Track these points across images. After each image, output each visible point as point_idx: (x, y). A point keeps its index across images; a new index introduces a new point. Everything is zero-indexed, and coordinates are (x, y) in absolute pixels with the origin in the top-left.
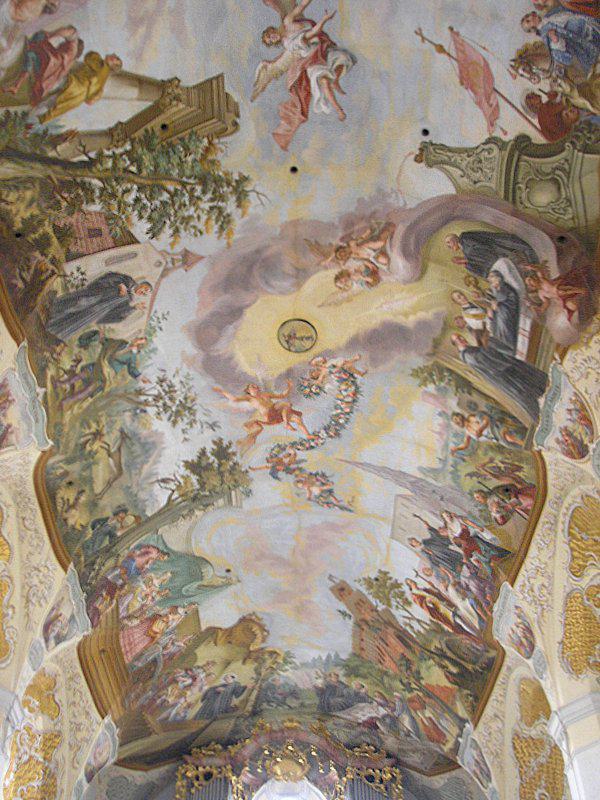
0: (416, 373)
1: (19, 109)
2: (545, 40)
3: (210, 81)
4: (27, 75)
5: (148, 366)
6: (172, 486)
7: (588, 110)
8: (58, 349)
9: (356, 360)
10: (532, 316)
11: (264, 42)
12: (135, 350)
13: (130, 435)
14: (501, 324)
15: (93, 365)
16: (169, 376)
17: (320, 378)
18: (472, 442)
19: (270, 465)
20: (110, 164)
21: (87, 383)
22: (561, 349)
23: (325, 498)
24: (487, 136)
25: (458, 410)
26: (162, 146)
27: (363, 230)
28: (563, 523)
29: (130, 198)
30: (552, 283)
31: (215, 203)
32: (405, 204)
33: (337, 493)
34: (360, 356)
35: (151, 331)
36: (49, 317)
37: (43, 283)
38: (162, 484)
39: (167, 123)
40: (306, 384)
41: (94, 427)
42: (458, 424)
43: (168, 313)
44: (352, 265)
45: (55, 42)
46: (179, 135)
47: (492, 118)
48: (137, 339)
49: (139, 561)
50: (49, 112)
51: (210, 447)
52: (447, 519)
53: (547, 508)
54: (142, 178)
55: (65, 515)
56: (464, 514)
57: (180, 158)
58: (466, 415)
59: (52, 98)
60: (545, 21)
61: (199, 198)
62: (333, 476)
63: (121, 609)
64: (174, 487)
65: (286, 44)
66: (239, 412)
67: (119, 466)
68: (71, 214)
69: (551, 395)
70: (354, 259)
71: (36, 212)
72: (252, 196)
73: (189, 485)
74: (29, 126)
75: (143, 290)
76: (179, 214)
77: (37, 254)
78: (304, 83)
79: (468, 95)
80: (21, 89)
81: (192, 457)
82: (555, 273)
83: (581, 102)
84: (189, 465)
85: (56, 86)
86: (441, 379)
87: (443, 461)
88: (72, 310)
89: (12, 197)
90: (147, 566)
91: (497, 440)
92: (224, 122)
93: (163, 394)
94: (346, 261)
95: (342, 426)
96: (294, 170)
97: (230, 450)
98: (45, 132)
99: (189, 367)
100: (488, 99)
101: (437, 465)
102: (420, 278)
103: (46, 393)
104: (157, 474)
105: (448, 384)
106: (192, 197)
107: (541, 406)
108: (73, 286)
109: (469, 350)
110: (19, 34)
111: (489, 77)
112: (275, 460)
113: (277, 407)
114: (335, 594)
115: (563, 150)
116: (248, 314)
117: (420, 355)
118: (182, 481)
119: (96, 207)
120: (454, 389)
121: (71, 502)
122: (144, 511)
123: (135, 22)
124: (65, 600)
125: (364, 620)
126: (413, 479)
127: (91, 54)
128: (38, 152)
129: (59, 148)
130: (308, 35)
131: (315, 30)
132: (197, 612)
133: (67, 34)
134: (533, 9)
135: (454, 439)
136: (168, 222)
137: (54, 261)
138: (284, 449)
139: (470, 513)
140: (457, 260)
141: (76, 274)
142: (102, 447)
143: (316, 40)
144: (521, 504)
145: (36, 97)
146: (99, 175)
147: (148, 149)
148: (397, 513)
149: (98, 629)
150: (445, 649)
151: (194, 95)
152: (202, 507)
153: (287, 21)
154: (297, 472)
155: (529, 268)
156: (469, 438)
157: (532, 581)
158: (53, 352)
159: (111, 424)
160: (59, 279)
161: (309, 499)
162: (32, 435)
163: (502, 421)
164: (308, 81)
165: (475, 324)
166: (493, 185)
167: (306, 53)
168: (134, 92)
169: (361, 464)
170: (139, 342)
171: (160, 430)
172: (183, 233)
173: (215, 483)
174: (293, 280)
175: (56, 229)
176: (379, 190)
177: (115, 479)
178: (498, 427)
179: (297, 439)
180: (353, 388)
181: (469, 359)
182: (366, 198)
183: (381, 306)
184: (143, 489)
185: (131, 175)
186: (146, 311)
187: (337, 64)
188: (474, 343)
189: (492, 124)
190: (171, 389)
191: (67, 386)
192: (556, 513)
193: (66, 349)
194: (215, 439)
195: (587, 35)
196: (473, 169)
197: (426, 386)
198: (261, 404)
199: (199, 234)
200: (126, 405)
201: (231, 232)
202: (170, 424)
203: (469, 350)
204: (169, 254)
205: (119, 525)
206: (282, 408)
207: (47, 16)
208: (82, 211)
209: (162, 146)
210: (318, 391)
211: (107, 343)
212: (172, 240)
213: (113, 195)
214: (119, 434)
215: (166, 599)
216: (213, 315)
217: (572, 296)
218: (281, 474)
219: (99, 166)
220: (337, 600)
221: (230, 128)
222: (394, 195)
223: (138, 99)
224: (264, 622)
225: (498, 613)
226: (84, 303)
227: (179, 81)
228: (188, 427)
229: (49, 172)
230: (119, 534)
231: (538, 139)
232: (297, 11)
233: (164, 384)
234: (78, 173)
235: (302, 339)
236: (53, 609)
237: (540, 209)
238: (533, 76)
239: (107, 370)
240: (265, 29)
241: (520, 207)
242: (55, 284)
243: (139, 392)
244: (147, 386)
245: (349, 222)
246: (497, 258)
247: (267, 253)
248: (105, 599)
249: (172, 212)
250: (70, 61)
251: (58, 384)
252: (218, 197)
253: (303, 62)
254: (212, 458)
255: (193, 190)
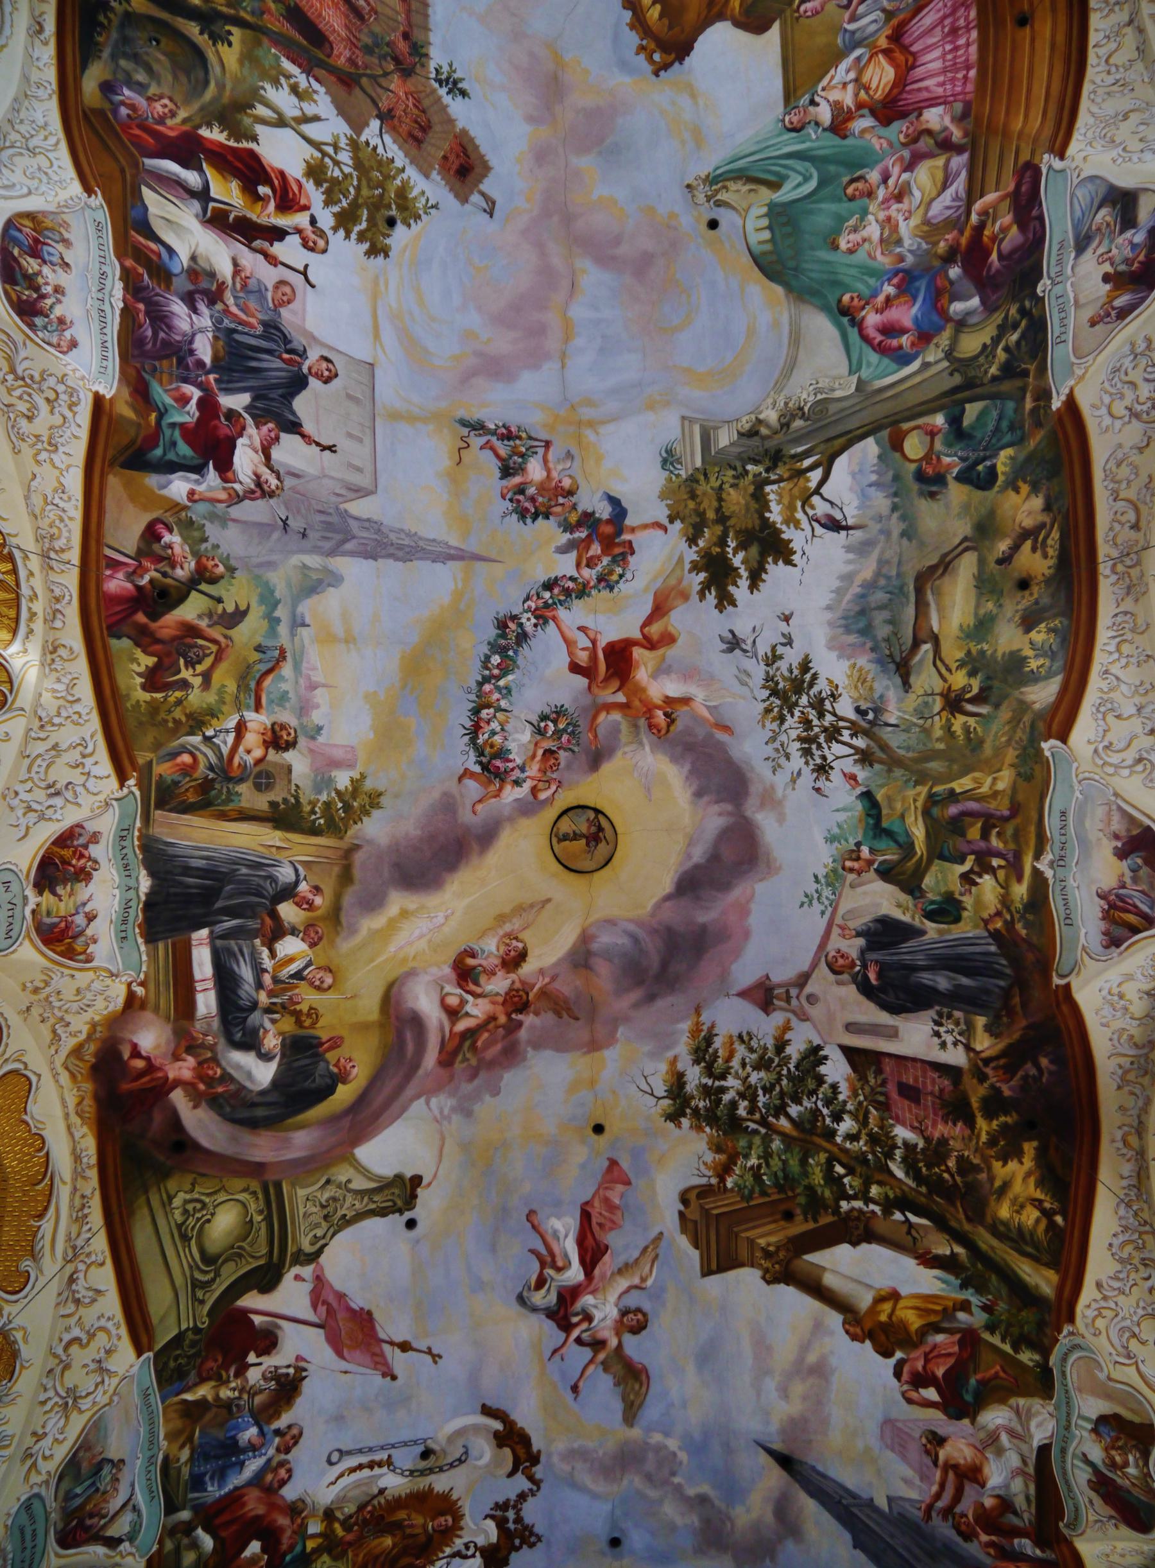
0: (374, 800)
1: (996, 1340)
2: (266, 1429)
3: (721, 1269)
4: (979, 1376)
5: (844, 809)
6: (820, 507)
7: (188, 1389)
8: (999, 924)
9: (480, 801)
10: (198, 1025)
11: (645, 1315)
12: (865, 851)
13: (892, 667)
14: (246, 973)
15: (942, 857)
16: (808, 777)
17: (540, 752)
18: (252, 702)
19: (626, 537)
20: (874, 1190)
21: (957, 825)
22: (137, 1004)
23: (515, 452)
24: (323, 1259)
25: (290, 756)
26: (793, 1190)
27: (488, 1045)
28: (31, 574)
29: (847, 1125)
30: (177, 1083)
31: (717, 1083)
32: (428, 1103)
33: (493, 466)
34: (474, 813)
35: (834, 879)
36: (1007, 994)
37: (1003, 1054)
38: (838, 516)
39: (782, 1223)
40: (565, 738)
41: (959, 722)
42: (283, 727)
43: (802, 905)
44: (499, 984)
45: (931, 1394)
46: (767, 1199)
47: (320, 1291)
48: (859, 873)
49: (907, 314)
50: (955, 1309)
51: (740, 591)
52: (266, 474)
53: (70, 580)
54: (826, 1151)
55: (1047, 519)
56: (236, 512)
57: (768, 1165)
58: (272, 755)
59: (946, 1325)
60: (271, 1451)
61: (742, 1095)
62: (504, 515)
63: (959, 185)
64: (816, 500)
65: (614, 1313)
66: (689, 674)
67: (921, 606)
68: (943, 1141)
69: (132, 911)
70: (497, 994)
71: (996, 1165)
72: (661, 1090)
73: (786, 501)
74: (985, 1308)
75: (841, 961)
76: (773, 1076)
77: (1007, 1092)
78: (588, 1260)
79: (358, 1301)
80: (991, 1368)
81: (776, 571)
82: (178, 1097)
83: (204, 1391)
84: (783, 552)
85: (940, 1338)
86: (328, 805)
87: (298, 623)
88: (965, 981)
89: (1031, 1216)
90: (889, 289)
91: (207, 740)
92: (702, 1207)
93: (822, 739)
94: (511, 990)
95: (495, 648)
96: (599, 1129)
97: (702, 576)
98: (964, 1286)
99: (772, 787)
100: (331, 1312)
101: (306, 608)
102: (390, 986)
103: (1037, 856)
104: (849, 549)
105: (313, 804)
106: (753, 1100)
107: (143, 872)
108: (957, 1024)
109: (288, 892)
110: (982, 1435)
111: (336, 1344)
112: (617, 551)
113: (616, 684)
114: (482, 157)
115: (209, 1314)
116: (667, 884)
117: (370, 842)
118: (799, 515)
119: (902, 1133)
120: (303, 800)
121: (1028, 544)
122: (880, 457)
123: (820, 1371)
124: (1088, 313)
125: (407, 72)
126: (348, 546)
127: (887, 1354)
128: (979, 1266)
129: (948, 1252)
130: (585, 1326)
131: (575, 1333)
132: (789, 95)
133: (913, 1395)
134: (289, 1457)
135: (284, 686)
136: (791, 1066)
137: (982, 1078)
138: (601, 579)
139: (223, 521)
140: (336, 1042)
141: (949, 1039)
142: (949, 670)
143: (575, 1320)
144: (130, 577)
145: (969, 1339)
146: (894, 1182)
147: (815, 1192)
148: (368, 440)
149: (1025, 156)
150: (202, 40)
151: (744, 1254)
152: (764, 431)
153: (613, 1342)
154: (573, 518)
155: (220, 1090)
156: (258, 707)
157: (57, 420)
158: (1009, 925)
159: (922, 712)
160: (978, 1048)
161: (548, 444)
162: (1077, 794)
163: (206, 786)
164: (582, 1261)
165: (290, 946)
166: (302, 1193)
167: (587, 1300)
168: (829, 1280)
169: (452, 558)
170: (856, 865)
171: (833, 655)
172: (770, 1043)
173: (731, 491)
174: (595, 946)
175: (970, 1123)
176: (468, 1114)
177: (933, 569)
178: (211, 768)
179: (578, 605)
180: (480, 741)
181: (285, 874)
182: (487, 1098)
183: (447, 917)
184: (879, 518)
185: (845, 1160)
186: (838, 920)
187: (543, 1291)
188: (288, 911)
189: (319, 1279)
190: (808, 743)
191: (995, 842)
192: (53, 577)
193: (985, 916)
194: (730, 608)
195: (212, 1478)
196: (335, 1199)
197: (352, 780)
198: (644, 690)
199: (746, 1038)
200: (894, 739)
201: (695, 1031)
202: (815, 666)
203: (288, 892)
204: (794, 1012)
205: (938, 445)
206: (607, 679)
207: (941, 1431)
208: (927, 1140)
209: (793, 1190)
210: (542, 724)
211: (911, 885)
212: (787, 1037)
213: (873, 1140)
214: (912, 680)
215: (856, 163)
216: (725, 886)
217: (142, 1074)
218: (604, 511)
219: (891, 1195)
220: (472, 133)
221: (692, 1196)
222: (446, 1111)
223: (824, 1269)
224: (633, 39)
225: (108, 282)
226: (942, 982)
227: (763, 1278)
228: (780, 650)
229: (967, 1227)
230: (939, 420)
231: (251, 1301)
232: (602, 1356)
233: (819, 761)
234: (923, 1199)
235: (576, 837)
236: (1123, 314)
237: (222, 1197)
238: (275, 1376)
239: (919, 832)
240: (644, 1333)
241: (255, 1185)
242: (986, 1044)
243: (865, 758)
244: (849, 765)
245: (511, 1055)
246: (275, 1083)
247: (635, 995)
248: (994, 238)
249: (785, 1082)
250: (916, 1359)
251: (1010, 856)
252: (713, 1094)
253: (592, 1288)
254: (737, 560)
255: (752, 1110)
